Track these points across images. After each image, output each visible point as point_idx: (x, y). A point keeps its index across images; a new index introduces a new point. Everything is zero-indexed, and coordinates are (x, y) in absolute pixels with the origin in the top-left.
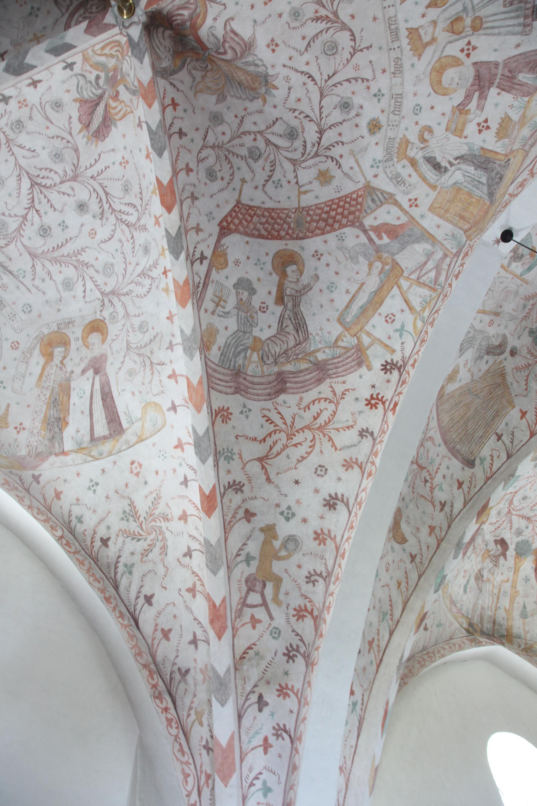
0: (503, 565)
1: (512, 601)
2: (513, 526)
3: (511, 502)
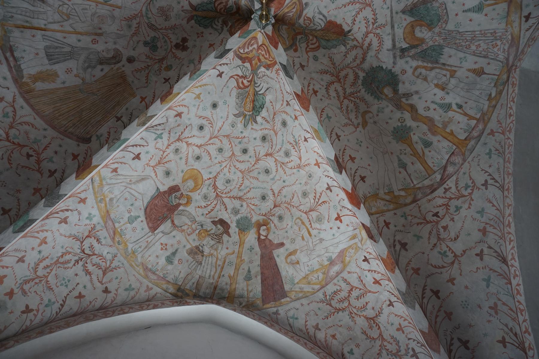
0: (228, 242)
1: (237, 269)
2: (228, 207)
3: (215, 187)
